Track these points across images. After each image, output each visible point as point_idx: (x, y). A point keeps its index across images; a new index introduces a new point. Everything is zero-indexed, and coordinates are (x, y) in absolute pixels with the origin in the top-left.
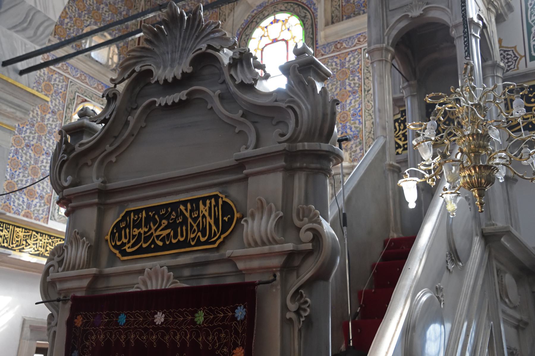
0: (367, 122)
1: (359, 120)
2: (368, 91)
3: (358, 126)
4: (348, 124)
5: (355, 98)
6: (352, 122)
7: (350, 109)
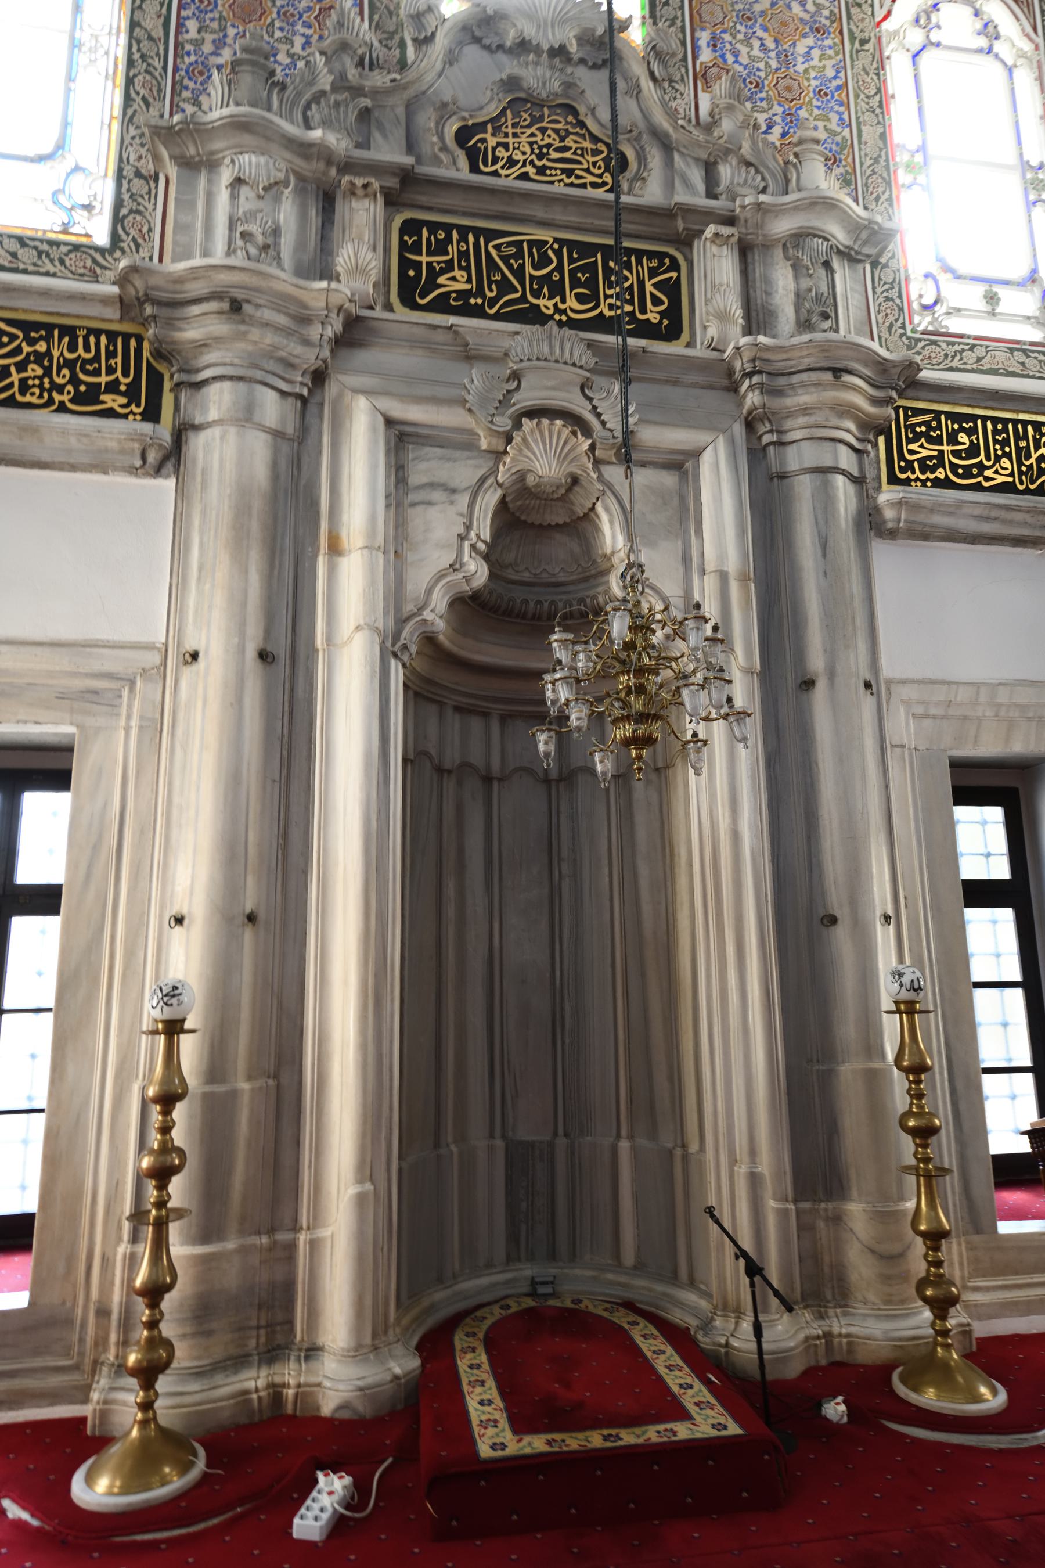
1: (840, 114)
2: (863, 42)
3: (839, 129)
6: (816, 112)
7: (806, 71)
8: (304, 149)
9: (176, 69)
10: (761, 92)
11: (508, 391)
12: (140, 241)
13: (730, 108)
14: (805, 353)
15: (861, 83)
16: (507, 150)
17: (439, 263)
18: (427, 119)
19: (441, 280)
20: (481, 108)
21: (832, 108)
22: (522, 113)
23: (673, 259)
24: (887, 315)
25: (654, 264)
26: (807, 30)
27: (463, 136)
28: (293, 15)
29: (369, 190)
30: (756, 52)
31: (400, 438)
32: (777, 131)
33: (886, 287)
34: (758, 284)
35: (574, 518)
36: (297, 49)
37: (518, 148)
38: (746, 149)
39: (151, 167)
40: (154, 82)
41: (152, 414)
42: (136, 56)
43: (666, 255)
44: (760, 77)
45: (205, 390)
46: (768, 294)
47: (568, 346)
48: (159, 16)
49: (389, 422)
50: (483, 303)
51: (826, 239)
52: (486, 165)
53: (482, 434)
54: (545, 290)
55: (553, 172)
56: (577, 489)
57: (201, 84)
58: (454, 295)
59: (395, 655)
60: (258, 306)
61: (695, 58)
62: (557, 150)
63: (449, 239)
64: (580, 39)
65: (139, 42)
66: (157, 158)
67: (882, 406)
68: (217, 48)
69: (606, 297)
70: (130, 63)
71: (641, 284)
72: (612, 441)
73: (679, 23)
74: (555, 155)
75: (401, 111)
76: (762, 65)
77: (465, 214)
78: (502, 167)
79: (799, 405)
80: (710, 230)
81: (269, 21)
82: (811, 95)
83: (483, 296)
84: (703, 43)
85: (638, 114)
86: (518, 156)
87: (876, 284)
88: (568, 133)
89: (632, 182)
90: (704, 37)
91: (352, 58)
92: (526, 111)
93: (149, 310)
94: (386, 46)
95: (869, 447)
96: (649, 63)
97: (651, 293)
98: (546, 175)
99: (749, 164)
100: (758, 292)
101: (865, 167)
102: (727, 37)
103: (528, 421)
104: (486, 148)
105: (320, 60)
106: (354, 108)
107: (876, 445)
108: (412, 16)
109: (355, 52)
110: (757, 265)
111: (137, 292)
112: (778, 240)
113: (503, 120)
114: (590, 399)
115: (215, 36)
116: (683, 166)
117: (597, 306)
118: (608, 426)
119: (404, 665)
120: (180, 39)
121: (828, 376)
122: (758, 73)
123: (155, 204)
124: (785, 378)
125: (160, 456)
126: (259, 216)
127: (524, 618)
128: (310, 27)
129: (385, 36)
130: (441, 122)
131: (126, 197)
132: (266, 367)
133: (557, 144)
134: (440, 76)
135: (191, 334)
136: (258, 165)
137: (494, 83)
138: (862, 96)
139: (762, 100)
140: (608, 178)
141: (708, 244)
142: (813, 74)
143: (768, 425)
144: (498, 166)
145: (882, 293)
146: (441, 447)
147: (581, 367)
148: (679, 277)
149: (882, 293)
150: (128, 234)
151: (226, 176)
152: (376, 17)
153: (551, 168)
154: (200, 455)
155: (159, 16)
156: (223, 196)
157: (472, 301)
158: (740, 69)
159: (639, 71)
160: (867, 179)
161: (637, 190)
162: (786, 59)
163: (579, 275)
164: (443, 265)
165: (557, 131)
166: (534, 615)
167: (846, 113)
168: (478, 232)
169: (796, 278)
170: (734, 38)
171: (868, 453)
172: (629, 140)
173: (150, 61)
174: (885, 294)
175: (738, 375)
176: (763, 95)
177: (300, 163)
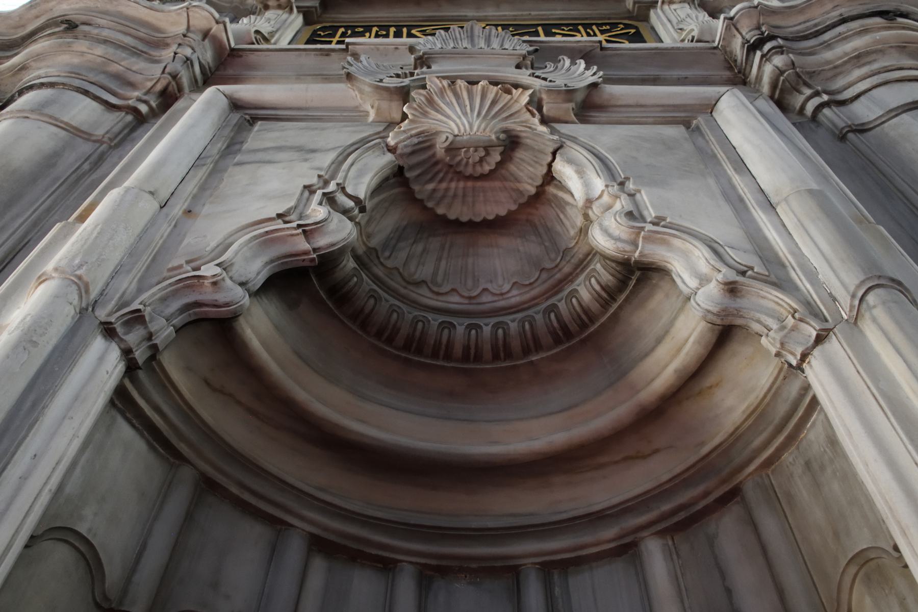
35: (523, 200)
56: (520, 154)
59: (109, 331)
79: (846, 54)
119: (127, 353)
127: (448, 357)
166: (467, 348)
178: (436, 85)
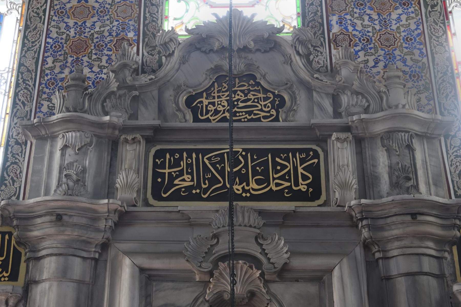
0: (435, 55)
2: (433, 6)
3: (420, 59)
4: (397, 52)
5: (407, 14)
6: (405, 50)
7: (398, 28)
8: (101, 125)
9: (40, 84)
10: (370, 44)
11: (212, 246)
12: (15, 178)
13: (345, 63)
14: (392, 206)
15: (433, 30)
16: (214, 106)
17: (175, 172)
18: (169, 94)
19: (176, 182)
20: (201, 84)
21: (415, 47)
22: (223, 84)
23: (315, 152)
24: (457, 166)
25: (303, 156)
26: (398, 5)
27: (189, 102)
28: (102, 46)
29: (136, 140)
30: (366, 22)
31: (147, 279)
32: (381, 64)
33: (455, 149)
34: (368, 161)
36: (104, 63)
37: (220, 104)
38: (356, 84)
39: (23, 138)
40: (29, 93)
41: (14, 277)
42: (21, 81)
43: (311, 149)
44: (369, 36)
45: (42, 261)
46: (374, 166)
47: (246, 215)
48: (33, 59)
49: (142, 270)
50: (200, 192)
51: (409, 132)
52: (202, 115)
53: (196, 272)
54: (237, 180)
55: (241, 114)
56: (255, 298)
57: (53, 90)
58: (183, 189)
60: (71, 216)
61: (329, 31)
62: (243, 102)
63: (181, 158)
64: (255, 41)
65: (22, 73)
66: (26, 136)
67: (451, 230)
68: (62, 69)
69: (274, 179)
70: (17, 85)
71: (295, 169)
72: (274, 270)
73: (319, 14)
74: (241, 105)
75: (155, 93)
76: (370, 29)
77: (191, 142)
78: (211, 116)
79: (393, 236)
80: (334, 136)
81: (90, 50)
82: (402, 41)
83: (200, 188)
84: (334, 23)
85: (291, 73)
86: (221, 108)
87: (449, 148)
88: (249, 91)
89: (287, 113)
90: (334, 19)
91: (129, 70)
92: (225, 83)
93: (15, 223)
94: (151, 54)
95: (446, 255)
96: (295, 47)
97: (301, 173)
98: (237, 116)
99: (357, 93)
100: (368, 166)
101: (438, 78)
102: (348, 17)
103: (222, 264)
104: (202, 106)
105: (112, 75)
106: (130, 96)
107: (451, 253)
108: (162, 45)
109: (131, 67)
110: (367, 149)
111: (10, 214)
112: (379, 134)
113: (212, 89)
114: (261, 245)
115: (62, 63)
116: (319, 99)
117: (269, 185)
118: (271, 261)
120: (43, 68)
121: (409, 218)
122: (367, 34)
123: (24, 158)
124: (383, 220)
125: (16, 300)
126: (75, 164)
128: (111, 51)
129: (150, 49)
130: (176, 97)
131: (10, 156)
132: (75, 246)
133: (243, 98)
134: (177, 70)
135: (36, 233)
136: (76, 137)
137: (208, 70)
138: (434, 37)
139: (371, 48)
140: (274, 112)
141: (335, 142)
142: (402, 29)
143: (377, 247)
144: (208, 115)
145: (453, 153)
146: (173, 281)
147: (255, 227)
148: (319, 162)
149: (453, 153)
150: (9, 176)
151: (60, 143)
152: (146, 40)
153: (239, 112)
154: (38, 298)
155: (33, 59)
156: (58, 154)
157: (194, 192)
158: (357, 33)
159: (290, 51)
160: (440, 85)
161: (291, 118)
162: (385, 23)
163: (258, 168)
164: (178, 173)
165: (242, 91)
167: (424, 48)
168: (198, 151)
169: (389, 157)
170: (353, 17)
171: (446, 258)
172: (285, 89)
173: (27, 82)
174: (455, 154)
175: (355, 220)
176: (372, 46)
177: (99, 131)
178: (223, 266)
